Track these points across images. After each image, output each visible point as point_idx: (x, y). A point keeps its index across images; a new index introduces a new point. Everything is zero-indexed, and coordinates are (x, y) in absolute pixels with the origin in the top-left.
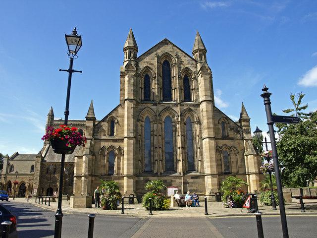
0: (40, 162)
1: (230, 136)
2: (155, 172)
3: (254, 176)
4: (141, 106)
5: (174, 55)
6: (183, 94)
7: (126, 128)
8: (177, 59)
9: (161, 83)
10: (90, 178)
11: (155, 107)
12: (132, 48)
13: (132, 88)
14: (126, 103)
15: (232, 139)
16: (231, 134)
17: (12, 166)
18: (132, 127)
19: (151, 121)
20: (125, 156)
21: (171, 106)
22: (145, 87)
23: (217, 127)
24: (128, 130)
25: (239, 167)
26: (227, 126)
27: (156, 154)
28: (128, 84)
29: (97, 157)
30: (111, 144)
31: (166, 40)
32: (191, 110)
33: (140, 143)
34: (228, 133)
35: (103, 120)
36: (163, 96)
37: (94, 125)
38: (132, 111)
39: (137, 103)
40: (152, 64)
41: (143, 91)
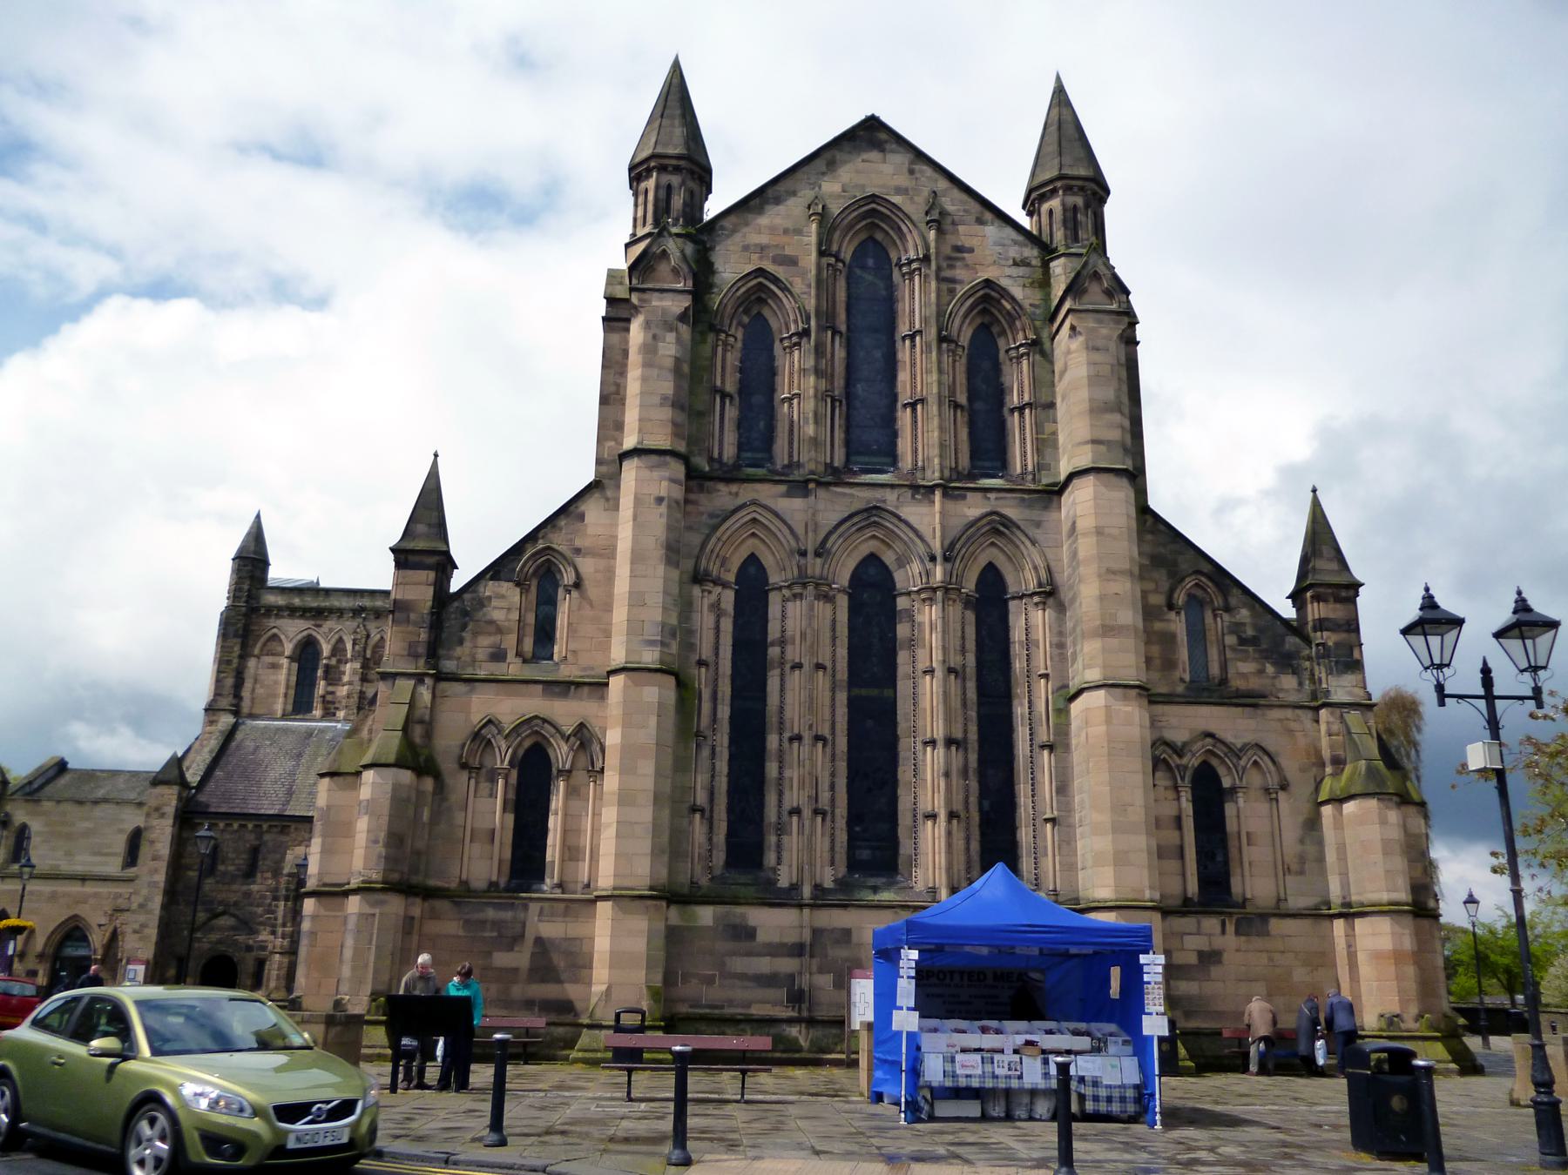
0: (170, 810)
1: (1236, 683)
2: (783, 882)
3: (1384, 925)
4: (724, 496)
5: (914, 207)
6: (964, 434)
7: (620, 615)
8: (932, 234)
9: (839, 369)
10: (395, 905)
11: (797, 503)
12: (677, 169)
13: (667, 387)
14: (631, 472)
15: (1251, 700)
16: (1245, 671)
18: (654, 615)
20: (611, 781)
21: (890, 497)
22: (744, 389)
23: (1158, 626)
24: (634, 627)
25: (1288, 870)
26: (1215, 624)
27: (793, 773)
28: (647, 364)
29: (449, 781)
30: (532, 704)
32: (1008, 523)
33: (706, 707)
34: (1224, 666)
35: (496, 570)
36: (848, 443)
37: (442, 597)
38: (658, 520)
39: (695, 479)
40: (792, 262)
41: (732, 413)
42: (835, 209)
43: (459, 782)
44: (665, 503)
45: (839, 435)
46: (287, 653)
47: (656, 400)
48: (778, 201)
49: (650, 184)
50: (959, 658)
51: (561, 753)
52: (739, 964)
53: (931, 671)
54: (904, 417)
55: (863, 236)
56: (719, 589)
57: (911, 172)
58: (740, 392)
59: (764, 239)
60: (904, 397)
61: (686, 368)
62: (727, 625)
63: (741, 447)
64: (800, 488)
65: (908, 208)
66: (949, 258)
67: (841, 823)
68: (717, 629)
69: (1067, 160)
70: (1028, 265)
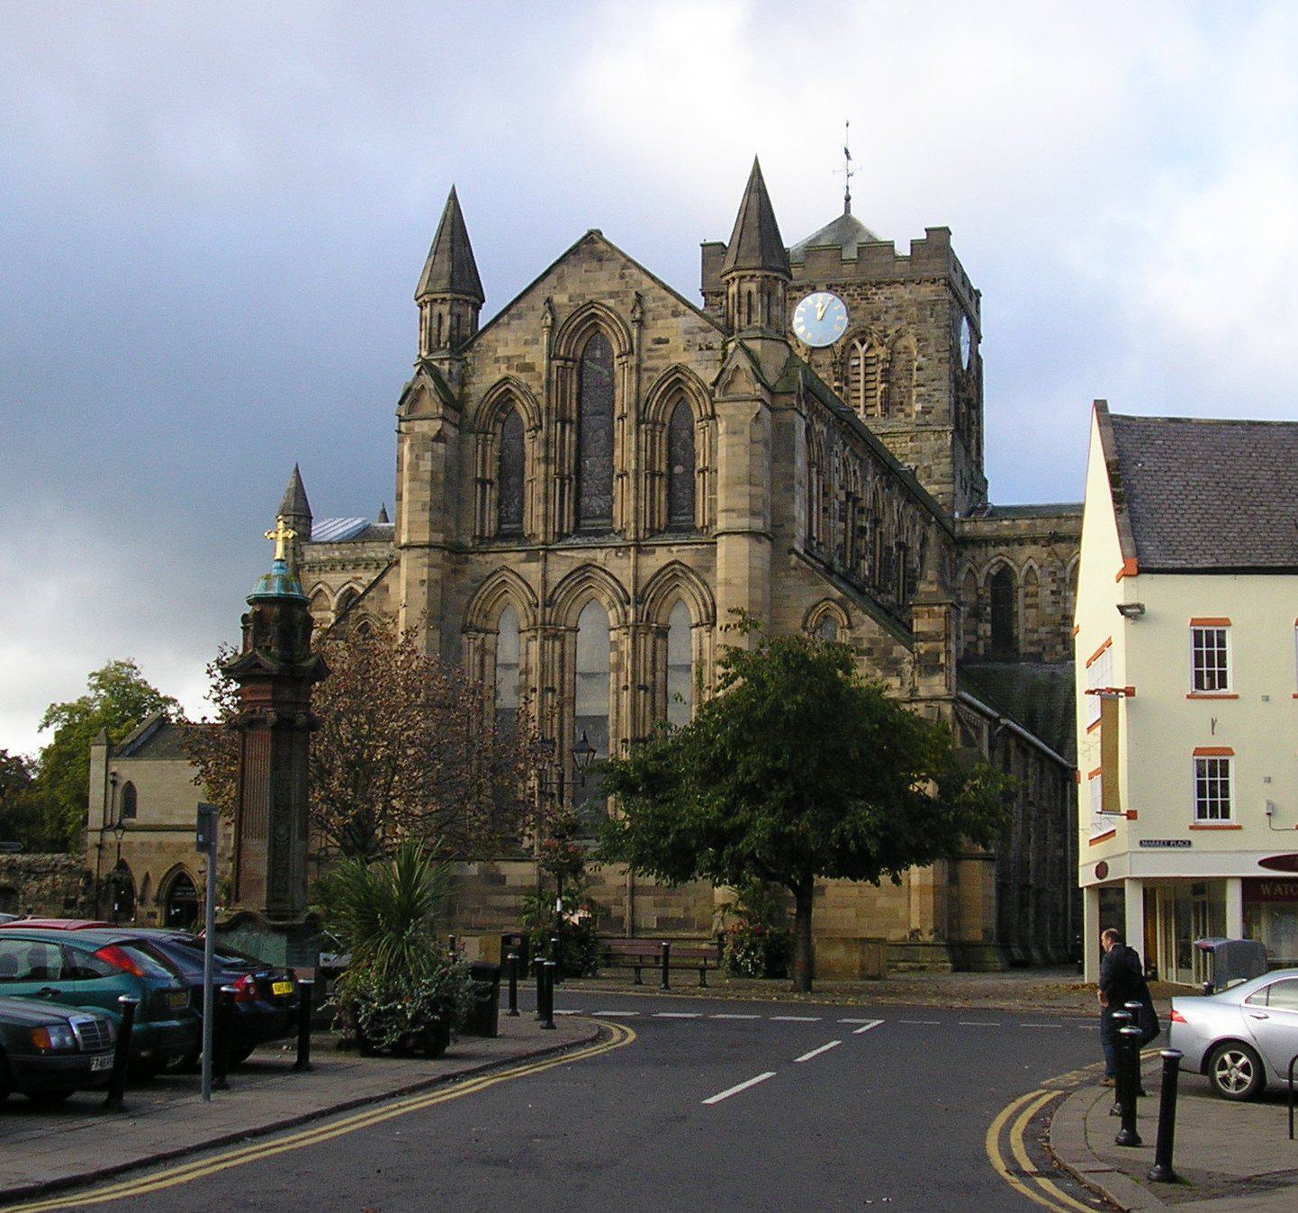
9: (570, 450)
13: (426, 495)
14: (405, 559)
17: (130, 790)
19: (523, 626)
21: (600, 556)
22: (503, 475)
28: (412, 480)
31: (592, 237)
40: (528, 368)
41: (492, 494)
42: (562, 318)
44: (426, 584)
45: (569, 506)
46: (333, 608)
47: (419, 506)
48: (520, 316)
49: (427, 311)
50: (649, 678)
52: (496, 901)
53: (626, 688)
54: (617, 485)
55: (592, 332)
56: (482, 635)
57: (622, 277)
58: (499, 477)
59: (510, 351)
60: (617, 471)
61: (441, 477)
63: (500, 521)
64: (531, 556)
65: (620, 309)
66: (650, 350)
68: (482, 664)
69: (744, 248)
70: (709, 348)
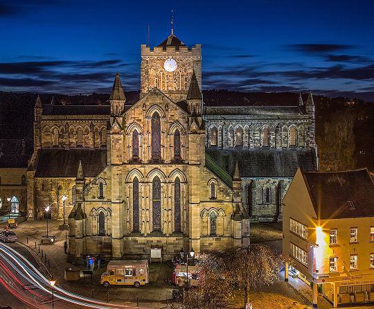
9: (150, 140)
27: (143, 215)
40: (140, 120)
43: (90, 218)
51: (105, 213)
52: (136, 246)
62: (132, 190)
67: (151, 223)
